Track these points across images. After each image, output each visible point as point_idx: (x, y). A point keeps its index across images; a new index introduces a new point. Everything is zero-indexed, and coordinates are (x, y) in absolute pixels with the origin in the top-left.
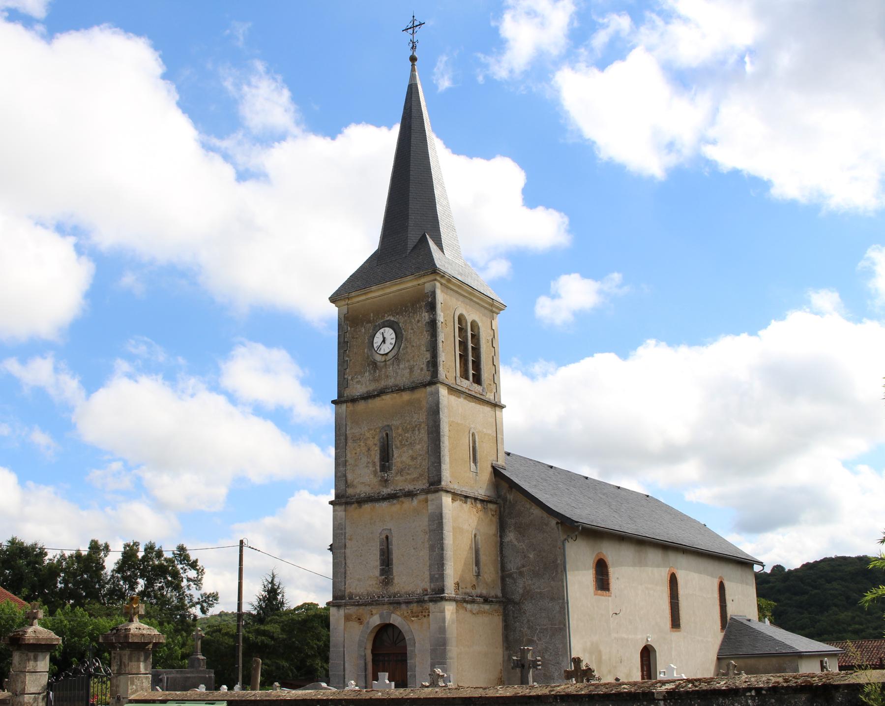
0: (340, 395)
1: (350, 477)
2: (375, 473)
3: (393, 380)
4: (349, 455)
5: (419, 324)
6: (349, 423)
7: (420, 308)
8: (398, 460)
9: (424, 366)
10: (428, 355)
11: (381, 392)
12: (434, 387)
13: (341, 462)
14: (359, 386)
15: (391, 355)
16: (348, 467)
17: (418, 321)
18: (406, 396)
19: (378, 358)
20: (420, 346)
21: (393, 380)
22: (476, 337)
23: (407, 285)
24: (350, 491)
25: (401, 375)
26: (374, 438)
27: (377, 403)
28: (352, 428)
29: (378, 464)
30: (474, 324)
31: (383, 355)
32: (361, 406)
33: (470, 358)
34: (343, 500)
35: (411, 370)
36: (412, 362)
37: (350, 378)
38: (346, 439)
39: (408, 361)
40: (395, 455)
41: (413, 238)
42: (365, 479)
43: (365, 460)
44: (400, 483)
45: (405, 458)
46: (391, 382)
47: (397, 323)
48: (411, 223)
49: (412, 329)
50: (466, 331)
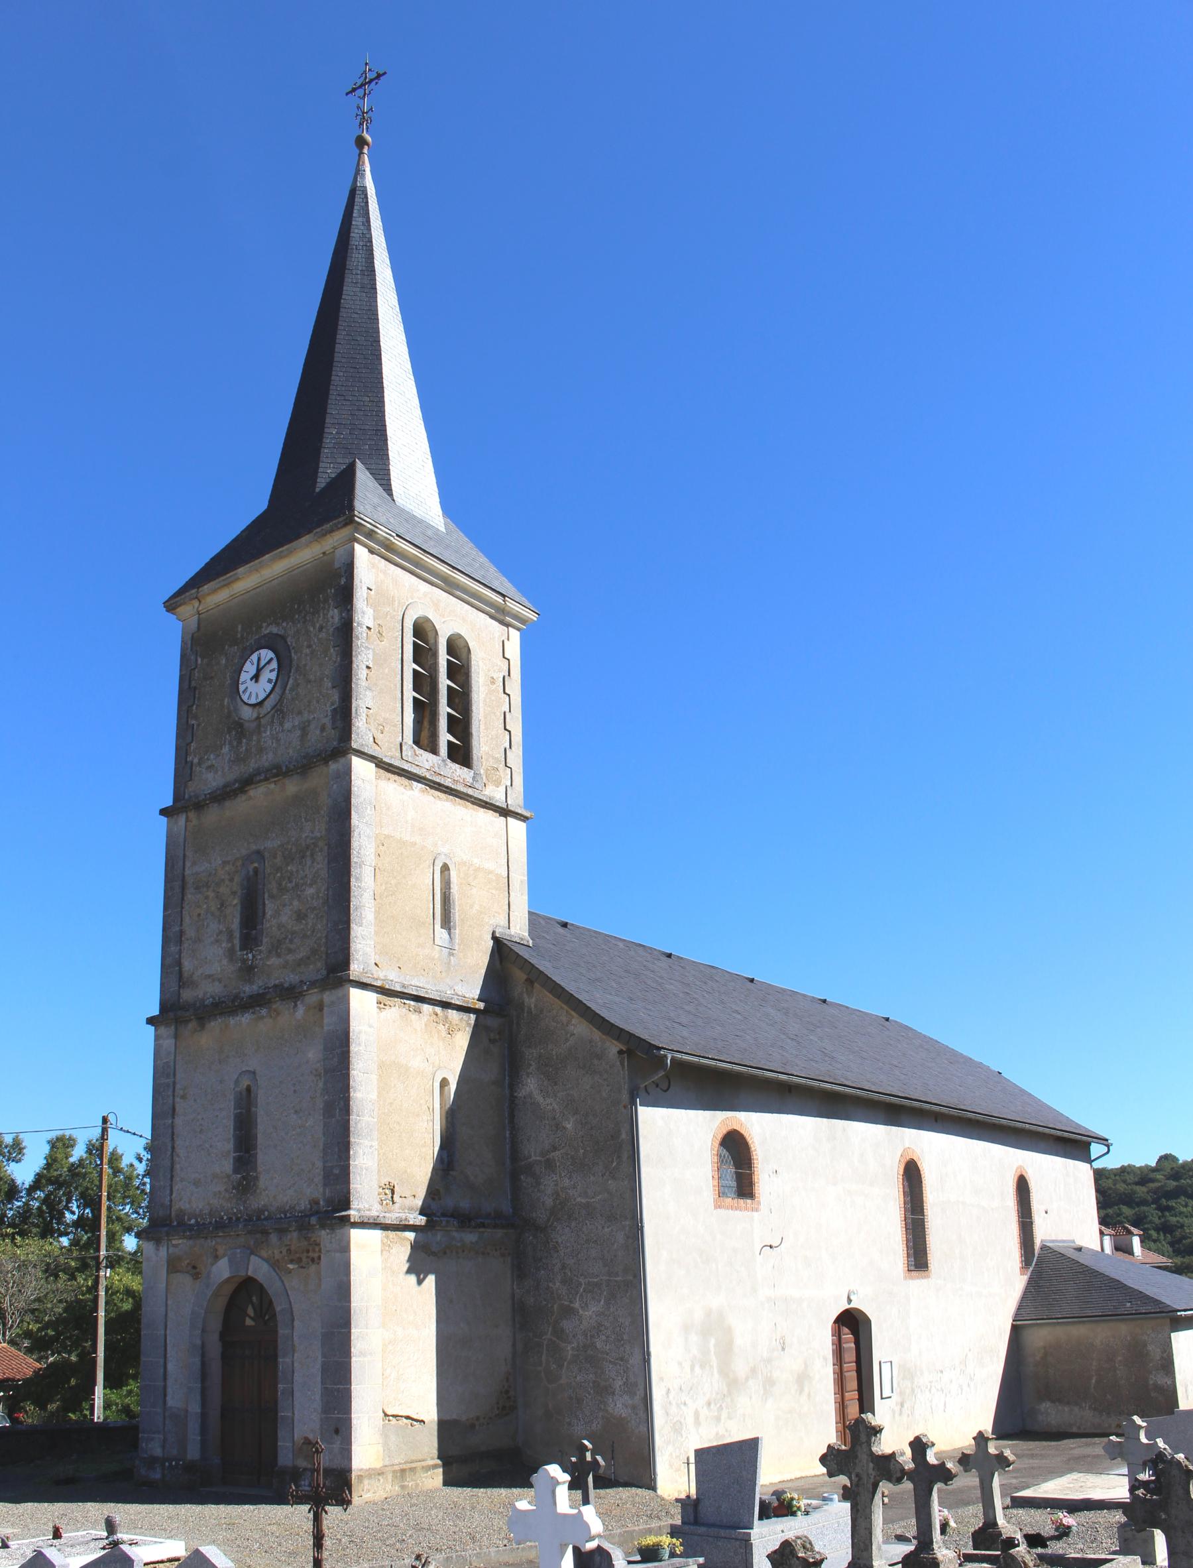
0: (177, 797)
1: (187, 965)
2: (231, 953)
3: (271, 756)
4: (187, 920)
5: (323, 635)
6: (189, 854)
7: (326, 601)
8: (274, 922)
9: (327, 721)
10: (336, 696)
11: (246, 783)
12: (342, 760)
13: (174, 937)
14: (210, 776)
15: (268, 705)
16: (186, 945)
17: (321, 628)
18: (292, 787)
19: (247, 713)
20: (321, 679)
21: (271, 756)
22: (460, 671)
23: (304, 554)
24: (187, 995)
25: (281, 743)
26: (231, 880)
27: (240, 807)
28: (194, 863)
29: (237, 934)
30: (457, 647)
31: (254, 706)
32: (213, 816)
33: (444, 709)
34: (171, 1015)
35: (304, 729)
36: (306, 716)
37: (196, 761)
38: (183, 888)
39: (300, 713)
40: (269, 913)
41: (328, 471)
42: (213, 966)
43: (214, 926)
44: (277, 969)
45: (285, 918)
46: (267, 759)
47: (283, 638)
48: (328, 441)
49: (309, 646)
50: (435, 655)
